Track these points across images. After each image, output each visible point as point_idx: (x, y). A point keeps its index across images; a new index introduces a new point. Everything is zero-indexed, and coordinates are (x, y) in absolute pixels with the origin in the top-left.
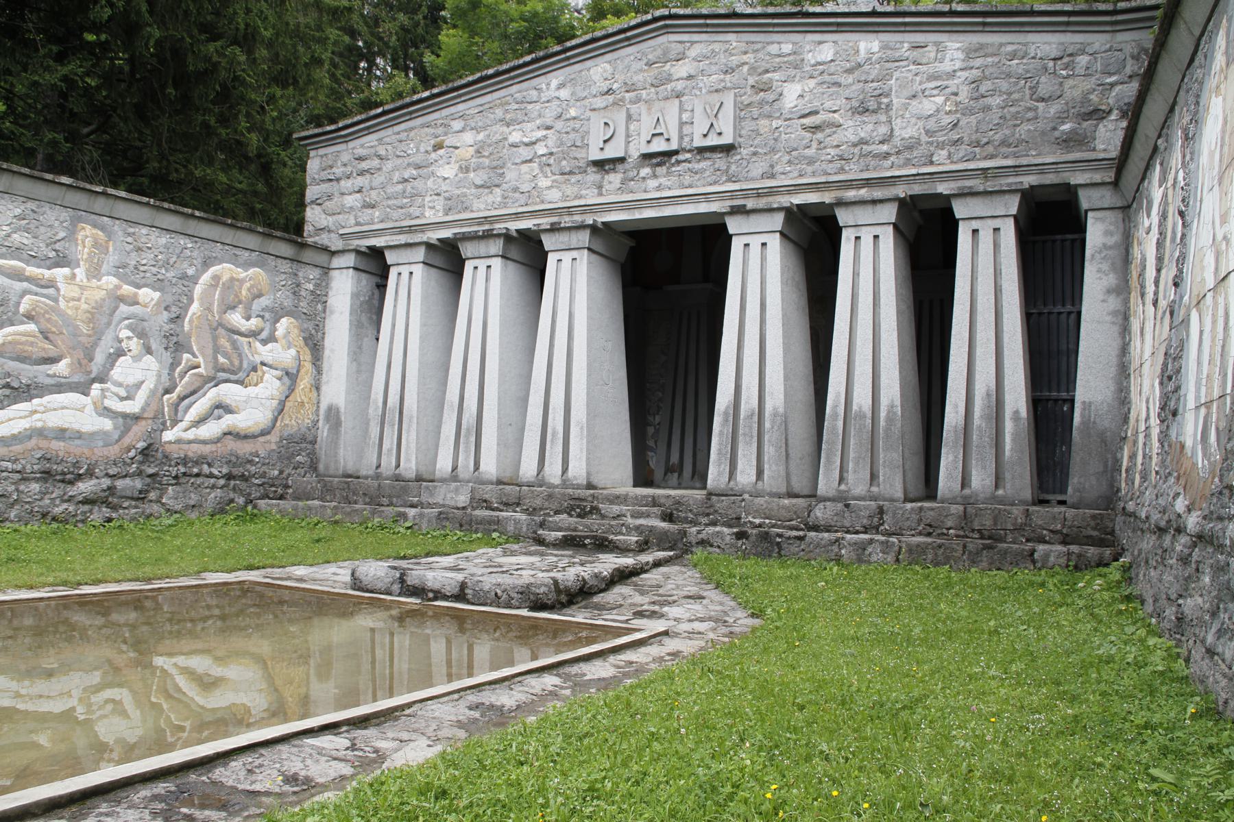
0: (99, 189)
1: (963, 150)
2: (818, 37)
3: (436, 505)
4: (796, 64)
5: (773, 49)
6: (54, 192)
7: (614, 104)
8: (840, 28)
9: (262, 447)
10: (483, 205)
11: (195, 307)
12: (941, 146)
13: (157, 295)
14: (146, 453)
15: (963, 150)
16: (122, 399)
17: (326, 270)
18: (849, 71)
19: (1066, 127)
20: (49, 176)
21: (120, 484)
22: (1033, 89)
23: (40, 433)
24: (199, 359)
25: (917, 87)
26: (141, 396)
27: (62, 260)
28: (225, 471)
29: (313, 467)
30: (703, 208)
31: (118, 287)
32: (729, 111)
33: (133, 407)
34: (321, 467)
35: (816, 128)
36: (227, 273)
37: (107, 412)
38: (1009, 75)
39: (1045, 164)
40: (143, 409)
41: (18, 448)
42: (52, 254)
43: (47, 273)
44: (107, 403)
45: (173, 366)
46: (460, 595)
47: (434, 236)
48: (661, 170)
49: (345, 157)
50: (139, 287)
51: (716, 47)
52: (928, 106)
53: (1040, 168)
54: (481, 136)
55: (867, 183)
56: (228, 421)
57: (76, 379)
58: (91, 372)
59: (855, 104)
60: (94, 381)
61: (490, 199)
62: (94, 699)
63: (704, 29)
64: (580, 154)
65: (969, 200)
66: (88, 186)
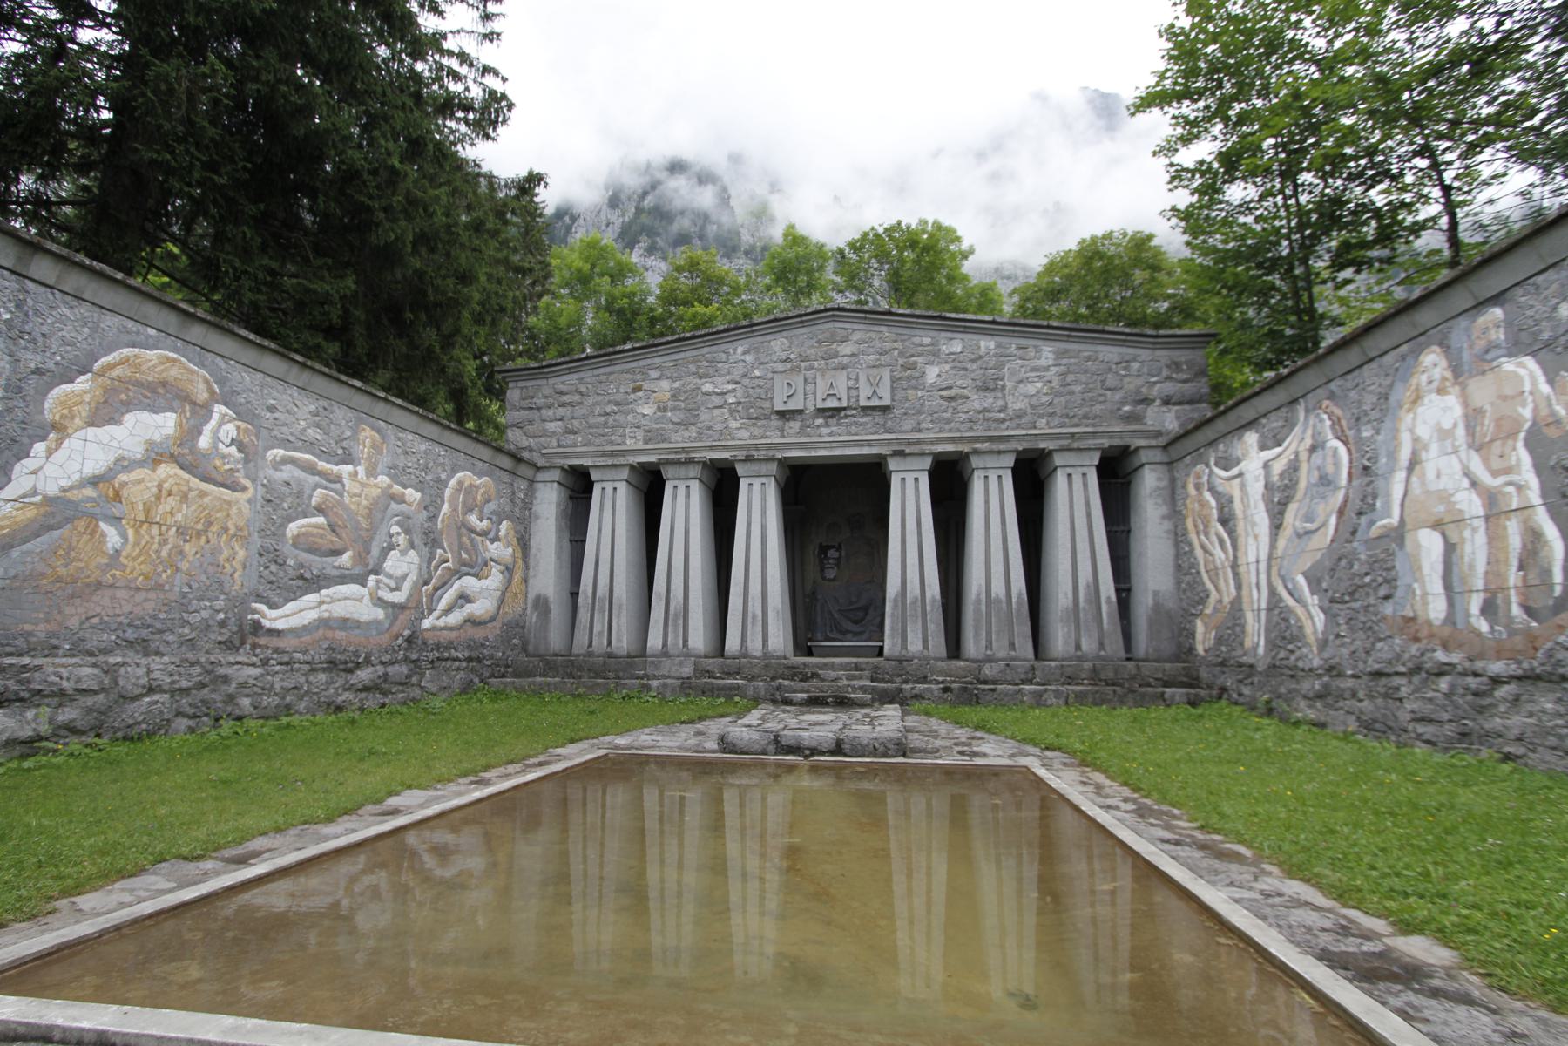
0: (382, 394)
1: (1057, 420)
2: (949, 335)
4: (934, 354)
5: (917, 340)
6: (345, 392)
7: (792, 369)
8: (966, 330)
9: (492, 632)
10: (681, 439)
11: (445, 508)
12: (1041, 416)
13: (418, 495)
14: (409, 640)
15: (1057, 420)
16: (392, 590)
17: (532, 482)
18: (973, 361)
19: (1127, 408)
20: (344, 378)
21: (391, 670)
22: (1103, 382)
23: (324, 623)
24: (447, 554)
25: (1022, 375)
26: (407, 586)
27: (348, 458)
28: (467, 654)
29: (524, 649)
30: (866, 451)
31: (390, 486)
33: (399, 597)
34: (531, 648)
35: (951, 399)
36: (468, 479)
37: (380, 602)
38: (1086, 372)
39: (1114, 433)
41: (307, 639)
42: (340, 451)
43: (335, 469)
44: (381, 593)
45: (431, 559)
46: (838, 749)
48: (833, 421)
49: (547, 391)
51: (873, 335)
52: (1031, 388)
53: (1110, 435)
54: (677, 385)
55: (991, 439)
56: (469, 609)
57: (356, 571)
59: (979, 383)
61: (686, 434)
63: (863, 321)
64: (767, 405)
65: (1067, 454)
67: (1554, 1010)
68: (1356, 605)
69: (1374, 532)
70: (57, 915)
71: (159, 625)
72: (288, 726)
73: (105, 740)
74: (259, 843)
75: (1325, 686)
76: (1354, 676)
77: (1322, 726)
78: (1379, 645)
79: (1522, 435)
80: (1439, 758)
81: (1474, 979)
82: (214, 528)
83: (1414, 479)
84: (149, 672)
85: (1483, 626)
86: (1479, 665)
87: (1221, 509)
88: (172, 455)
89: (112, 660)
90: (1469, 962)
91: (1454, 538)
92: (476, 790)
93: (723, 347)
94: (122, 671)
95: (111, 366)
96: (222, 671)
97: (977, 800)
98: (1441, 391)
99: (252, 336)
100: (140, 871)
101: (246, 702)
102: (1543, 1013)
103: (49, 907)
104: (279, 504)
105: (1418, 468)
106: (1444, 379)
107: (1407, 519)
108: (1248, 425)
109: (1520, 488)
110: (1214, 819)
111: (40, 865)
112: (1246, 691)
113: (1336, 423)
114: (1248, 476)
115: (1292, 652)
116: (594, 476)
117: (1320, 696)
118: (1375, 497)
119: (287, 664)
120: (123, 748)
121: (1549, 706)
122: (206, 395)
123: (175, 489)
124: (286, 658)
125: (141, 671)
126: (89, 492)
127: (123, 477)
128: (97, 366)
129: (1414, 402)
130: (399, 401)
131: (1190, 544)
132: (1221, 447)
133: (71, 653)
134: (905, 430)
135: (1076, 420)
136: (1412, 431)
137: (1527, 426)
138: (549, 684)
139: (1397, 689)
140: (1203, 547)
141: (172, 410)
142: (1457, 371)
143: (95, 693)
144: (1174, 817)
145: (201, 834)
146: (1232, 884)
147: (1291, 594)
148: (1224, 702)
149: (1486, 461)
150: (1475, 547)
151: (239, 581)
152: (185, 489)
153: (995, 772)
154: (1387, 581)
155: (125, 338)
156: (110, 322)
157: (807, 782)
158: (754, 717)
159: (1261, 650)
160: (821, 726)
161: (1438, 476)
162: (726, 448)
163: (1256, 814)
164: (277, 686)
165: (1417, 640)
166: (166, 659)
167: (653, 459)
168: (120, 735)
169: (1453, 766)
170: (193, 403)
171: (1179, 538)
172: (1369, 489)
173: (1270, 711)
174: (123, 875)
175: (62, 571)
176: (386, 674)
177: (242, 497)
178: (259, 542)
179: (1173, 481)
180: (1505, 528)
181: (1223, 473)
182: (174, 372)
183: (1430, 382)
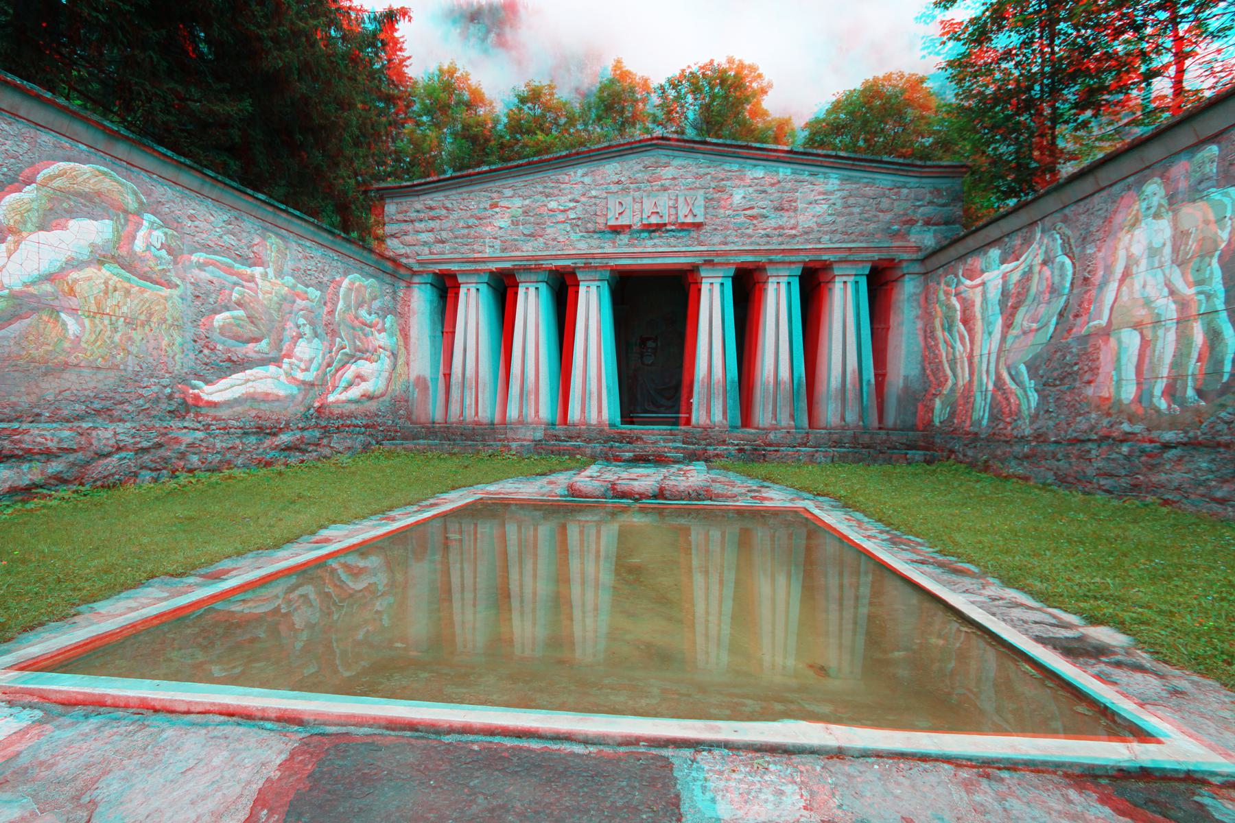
0: (283, 207)
1: (838, 236)
3: (519, 439)
7: (623, 190)
10: (529, 249)
11: (341, 305)
12: (826, 233)
13: (318, 293)
14: (319, 410)
15: (838, 236)
16: (303, 370)
18: (773, 185)
19: (895, 227)
20: (249, 191)
21: (306, 434)
23: (252, 398)
27: (258, 261)
29: (409, 418)
30: (682, 260)
31: (295, 286)
32: (701, 202)
33: (309, 377)
34: (414, 417)
35: (754, 217)
38: (863, 196)
40: (316, 378)
41: (239, 409)
42: (252, 255)
43: (249, 271)
46: (660, 494)
47: (493, 266)
49: (418, 206)
50: (307, 286)
54: (527, 202)
58: (281, 350)
59: (776, 204)
60: (285, 356)
61: (535, 244)
62: (292, 596)
65: (844, 266)
66: (276, 203)
67: (1203, 675)
68: (1064, 388)
69: (1084, 331)
70: (82, 616)
71: (118, 397)
72: (230, 477)
73: (88, 487)
74: (226, 564)
75: (1032, 449)
76: (1055, 442)
77: (1026, 479)
78: (1079, 419)
79: (1218, 253)
80: (1115, 502)
81: (1145, 655)
82: (154, 319)
83: (1124, 288)
84: (116, 434)
85: (1163, 405)
86: (1155, 434)
87: (964, 311)
88: (113, 257)
89: (84, 425)
90: (1140, 643)
91: (1149, 335)
92: (386, 524)
93: (565, 170)
94: (94, 433)
95: (52, 178)
96: (173, 435)
97: (760, 535)
98: (1157, 216)
99: (169, 153)
100: (138, 584)
101: (195, 458)
102: (1196, 678)
103: (73, 611)
104: (205, 301)
105: (1128, 281)
106: (1160, 205)
107: (1114, 321)
108: (991, 244)
109: (1209, 296)
110: (951, 548)
111: (59, 581)
112: (970, 453)
113: (1066, 241)
114: (990, 286)
115: (1010, 423)
116: (460, 280)
117: (1027, 457)
118: (1090, 303)
119: (224, 429)
120: (104, 494)
121: (1204, 465)
122: (136, 205)
123: (119, 285)
124: (223, 425)
125: (109, 434)
126: (47, 287)
127: (74, 275)
128: (39, 178)
129: (1133, 225)
130: (297, 213)
131: (936, 339)
132: (969, 261)
133: (51, 419)
134: (713, 242)
135: (853, 237)
136: (1127, 250)
137: (1223, 245)
138: (429, 445)
139: (1089, 451)
140: (946, 342)
141: (109, 218)
142: (1172, 199)
143: (75, 451)
144: (918, 544)
145: (180, 557)
146: (966, 591)
147: (1013, 379)
148: (951, 461)
151: (182, 361)
152: (127, 285)
153: (776, 513)
154: (1091, 369)
155: (60, 152)
156: (46, 138)
157: (638, 520)
158: (593, 470)
159: (985, 422)
160: (645, 479)
161: (1144, 286)
162: (568, 256)
163: (980, 542)
164: (219, 445)
165: (1109, 415)
166: (128, 425)
167: (508, 265)
168: (99, 483)
169: (1126, 508)
170: (126, 212)
171: (928, 333)
172: (1087, 297)
173: (986, 468)
174: (126, 587)
175: (34, 353)
176: (302, 437)
177: (176, 293)
178: (193, 330)
179: (926, 288)
180: (1192, 328)
181: (968, 282)
182: (107, 184)
183: (1148, 208)
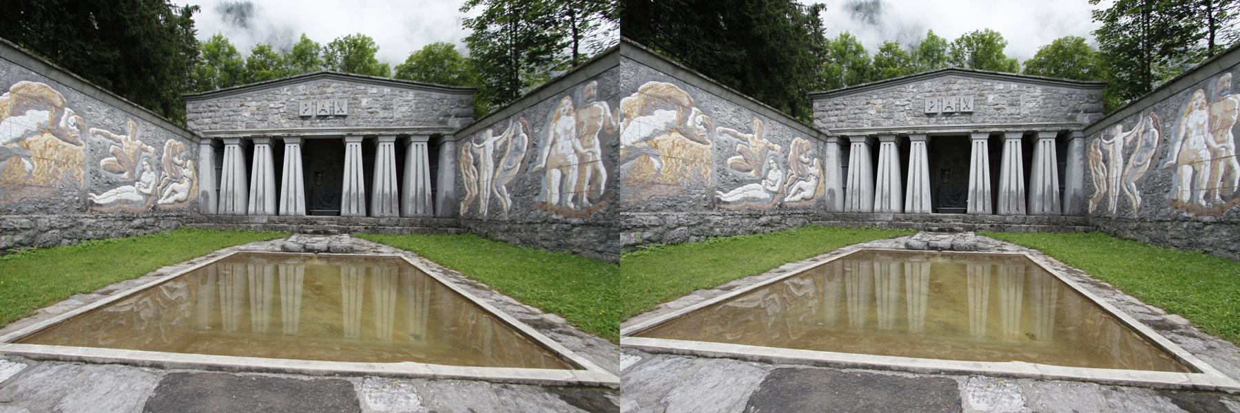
85: (572, 206)
98: (568, 114)
142: (575, 106)
149: (582, 143)
150: (573, 176)
